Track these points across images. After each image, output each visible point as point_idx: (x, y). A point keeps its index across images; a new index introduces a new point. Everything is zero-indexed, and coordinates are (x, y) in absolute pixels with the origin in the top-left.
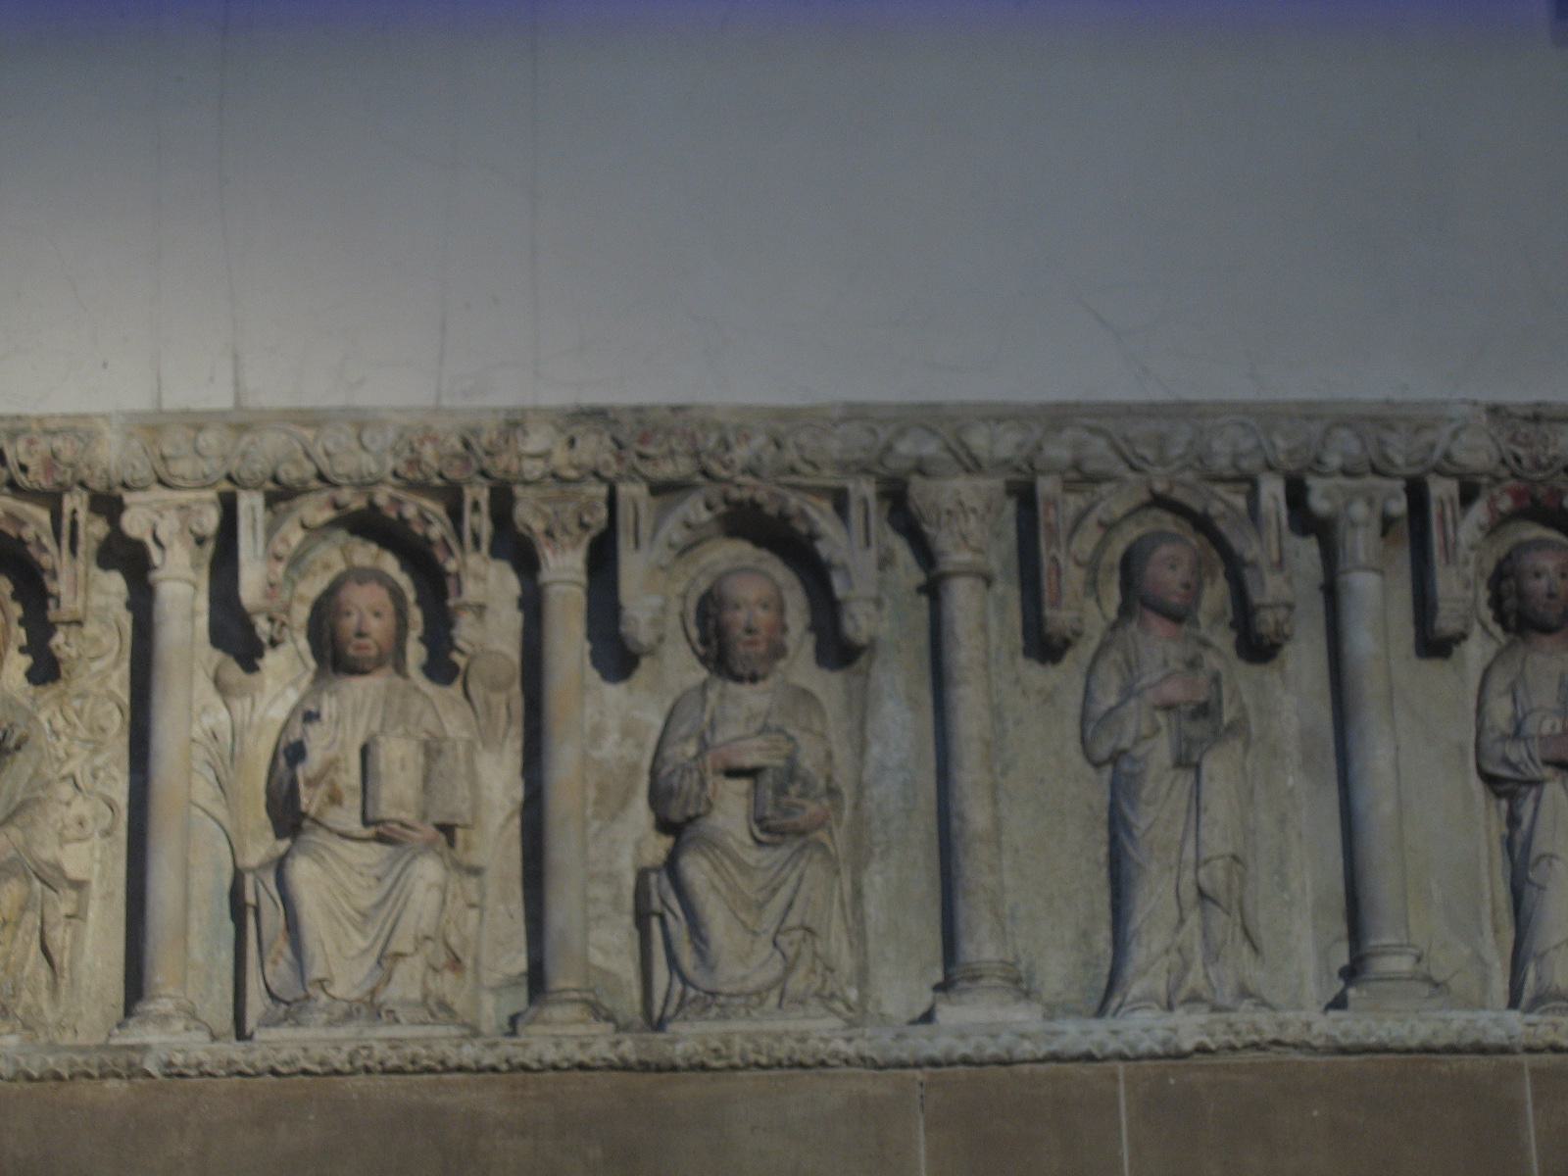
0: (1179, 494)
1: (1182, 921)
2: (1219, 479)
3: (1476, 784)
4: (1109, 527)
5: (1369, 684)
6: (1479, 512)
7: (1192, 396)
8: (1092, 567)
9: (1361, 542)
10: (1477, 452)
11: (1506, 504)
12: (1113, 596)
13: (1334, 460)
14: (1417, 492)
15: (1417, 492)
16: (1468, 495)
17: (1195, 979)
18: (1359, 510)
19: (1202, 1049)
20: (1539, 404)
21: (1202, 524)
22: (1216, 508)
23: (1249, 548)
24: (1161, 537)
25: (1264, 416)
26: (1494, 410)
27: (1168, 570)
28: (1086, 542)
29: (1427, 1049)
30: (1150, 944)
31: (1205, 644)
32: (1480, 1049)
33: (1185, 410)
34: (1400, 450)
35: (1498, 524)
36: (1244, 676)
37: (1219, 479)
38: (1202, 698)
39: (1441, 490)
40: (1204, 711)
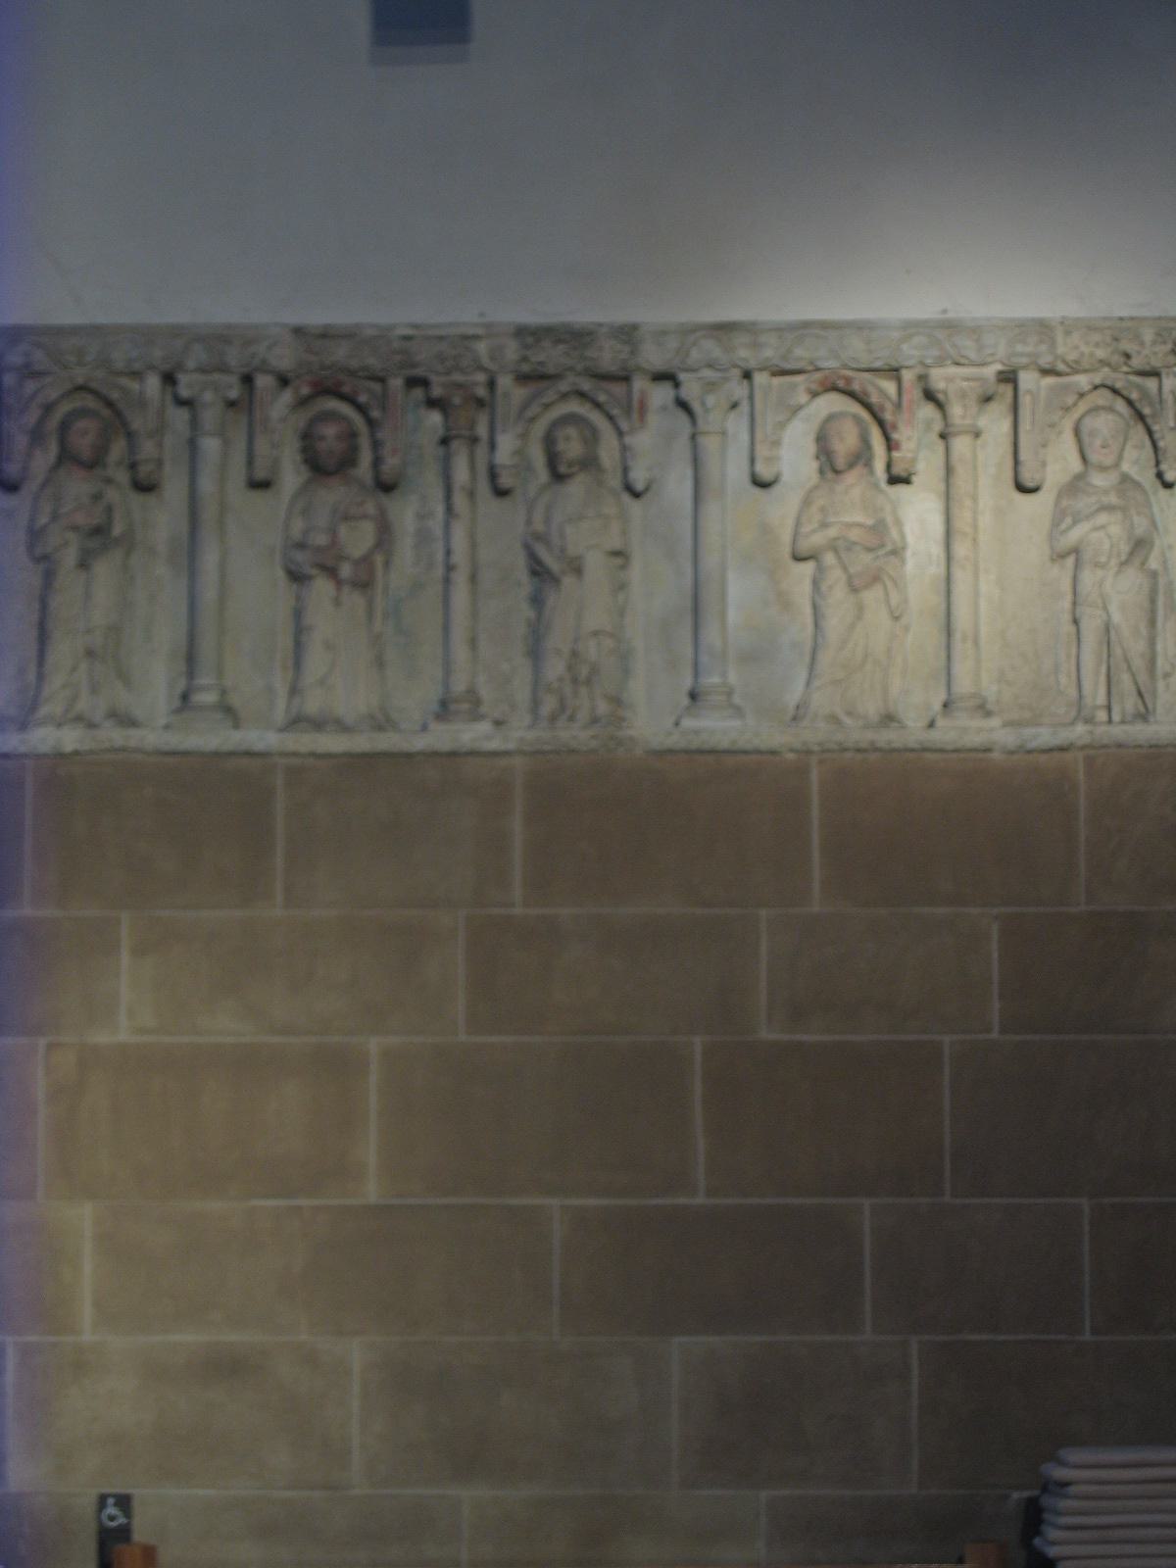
0: (94, 385)
1: (74, 669)
2: (121, 374)
3: (280, 574)
4: (48, 408)
5: (209, 513)
6: (287, 397)
7: (101, 318)
8: (37, 436)
9: (210, 417)
10: (284, 358)
11: (305, 391)
12: (53, 449)
13: (191, 364)
14: (248, 380)
15: (248, 380)
16: (284, 381)
17: (83, 705)
18: (208, 396)
19: (76, 753)
20: (327, 327)
21: (110, 404)
22: (115, 395)
23: (137, 423)
24: (83, 413)
25: (146, 334)
26: (298, 331)
27: (84, 438)
28: (32, 417)
29: (217, 755)
30: (56, 681)
31: (109, 481)
32: (249, 754)
33: (95, 330)
34: (233, 357)
35: (302, 402)
36: (136, 499)
37: (121, 374)
38: (96, 522)
39: (263, 381)
40: (99, 531)
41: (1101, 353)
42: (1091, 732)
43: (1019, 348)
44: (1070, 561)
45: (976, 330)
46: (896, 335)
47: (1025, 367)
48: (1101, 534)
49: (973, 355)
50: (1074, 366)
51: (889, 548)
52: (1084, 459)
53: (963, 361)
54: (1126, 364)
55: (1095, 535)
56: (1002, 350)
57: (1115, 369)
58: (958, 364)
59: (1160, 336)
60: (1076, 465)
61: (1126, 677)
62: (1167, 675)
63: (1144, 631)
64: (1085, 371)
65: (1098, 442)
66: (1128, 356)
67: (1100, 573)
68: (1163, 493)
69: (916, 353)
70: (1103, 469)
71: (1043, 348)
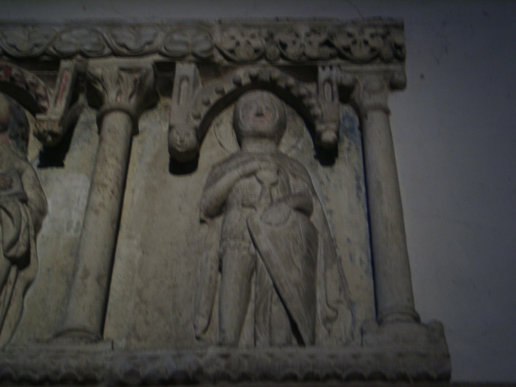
41: (257, 43)
42: (226, 356)
43: (176, 37)
44: (219, 221)
45: (136, 27)
46: (58, 30)
47: (182, 57)
48: (253, 180)
49: (131, 45)
50: (229, 55)
51: (16, 188)
52: (240, 141)
53: (124, 51)
54: (282, 56)
55: (246, 182)
56: (159, 41)
57: (271, 62)
58: (115, 54)
59: (314, 31)
60: (232, 146)
61: (277, 309)
62: (328, 320)
63: (297, 260)
64: (243, 63)
65: (252, 114)
66: (284, 46)
67: (248, 211)
68: (322, 170)
69: (74, 40)
70: (260, 136)
71: (201, 37)
